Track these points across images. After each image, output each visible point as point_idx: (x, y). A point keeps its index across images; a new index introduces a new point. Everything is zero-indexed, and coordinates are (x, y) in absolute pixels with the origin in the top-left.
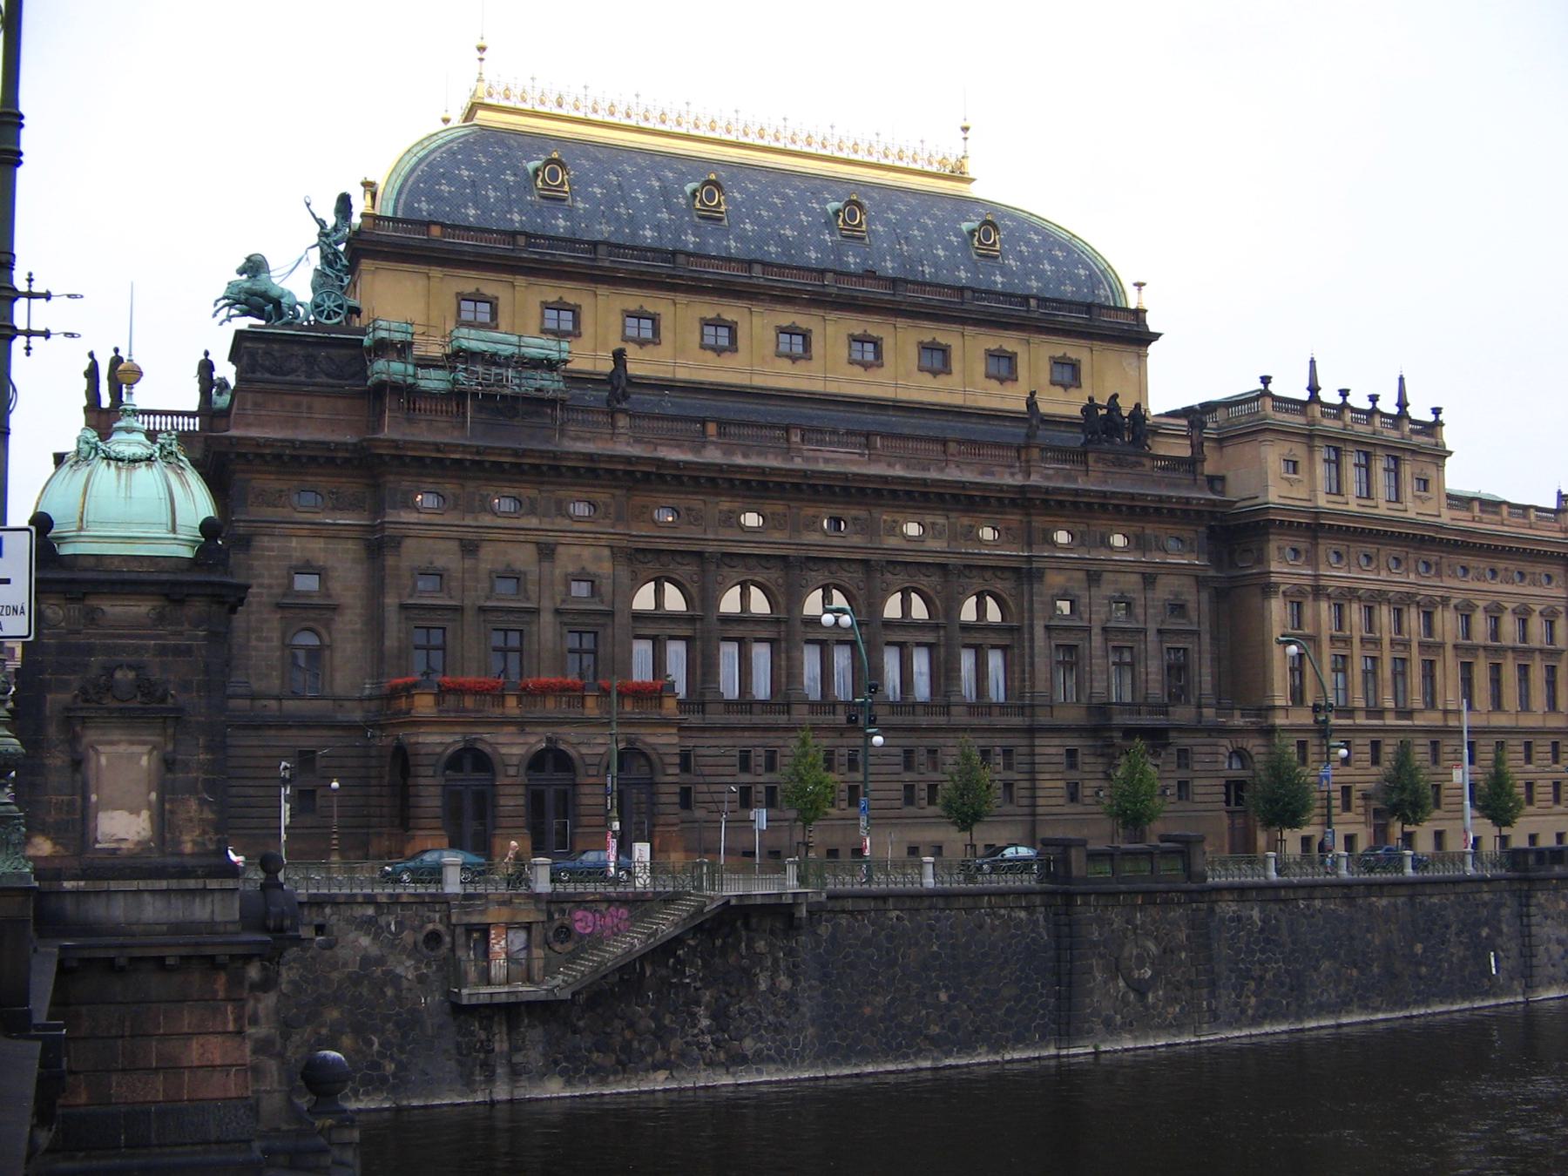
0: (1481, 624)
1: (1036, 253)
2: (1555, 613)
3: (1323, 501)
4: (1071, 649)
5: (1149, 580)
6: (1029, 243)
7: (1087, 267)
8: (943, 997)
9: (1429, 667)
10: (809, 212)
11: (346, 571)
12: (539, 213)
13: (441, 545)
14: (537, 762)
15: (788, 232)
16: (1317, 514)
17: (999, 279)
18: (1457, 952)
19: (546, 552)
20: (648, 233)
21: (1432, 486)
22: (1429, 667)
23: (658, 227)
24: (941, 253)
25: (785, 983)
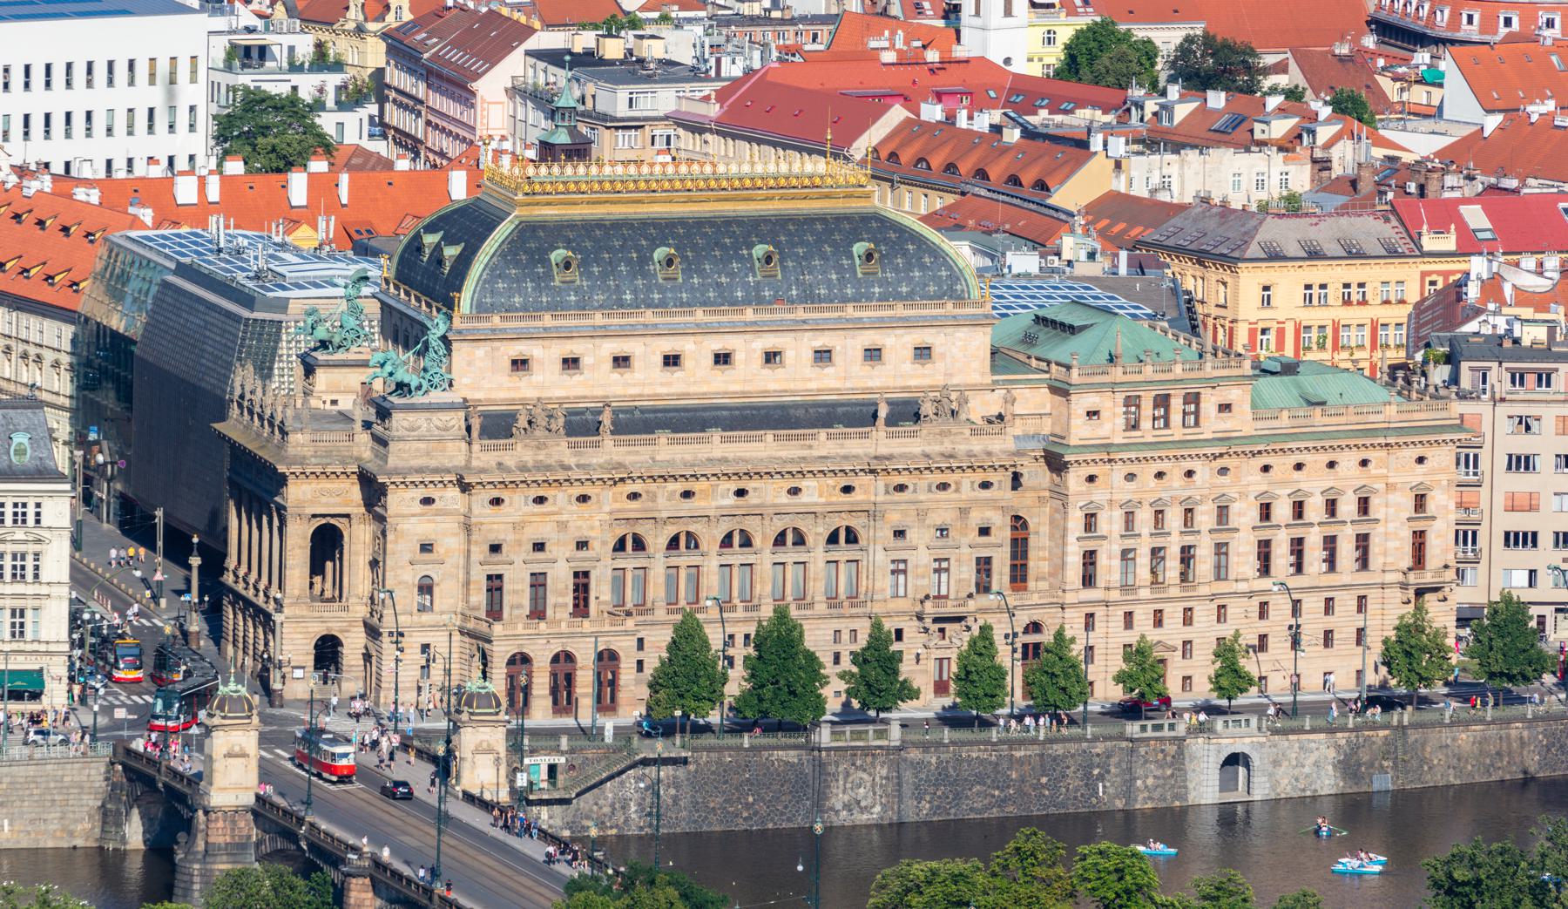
0: (1282, 512)
1: (909, 263)
2: (1376, 492)
3: (1118, 440)
4: (905, 561)
5: (964, 512)
6: (905, 253)
7: (949, 268)
8: (751, 799)
9: (1221, 549)
10: (740, 259)
11: (450, 543)
12: (559, 294)
13: (502, 527)
14: (555, 659)
15: (723, 280)
16: (1107, 447)
17: (877, 290)
18: (1074, 783)
19: (562, 526)
20: (628, 297)
21: (1234, 408)
22: (1221, 549)
23: (635, 292)
24: (834, 277)
25: (672, 791)
